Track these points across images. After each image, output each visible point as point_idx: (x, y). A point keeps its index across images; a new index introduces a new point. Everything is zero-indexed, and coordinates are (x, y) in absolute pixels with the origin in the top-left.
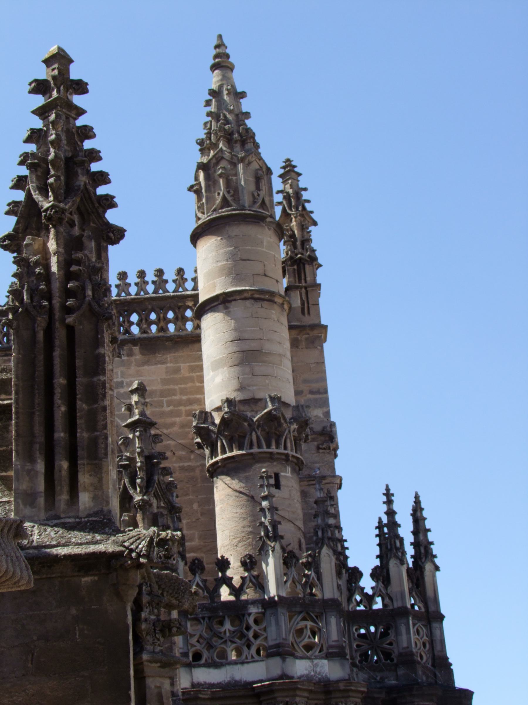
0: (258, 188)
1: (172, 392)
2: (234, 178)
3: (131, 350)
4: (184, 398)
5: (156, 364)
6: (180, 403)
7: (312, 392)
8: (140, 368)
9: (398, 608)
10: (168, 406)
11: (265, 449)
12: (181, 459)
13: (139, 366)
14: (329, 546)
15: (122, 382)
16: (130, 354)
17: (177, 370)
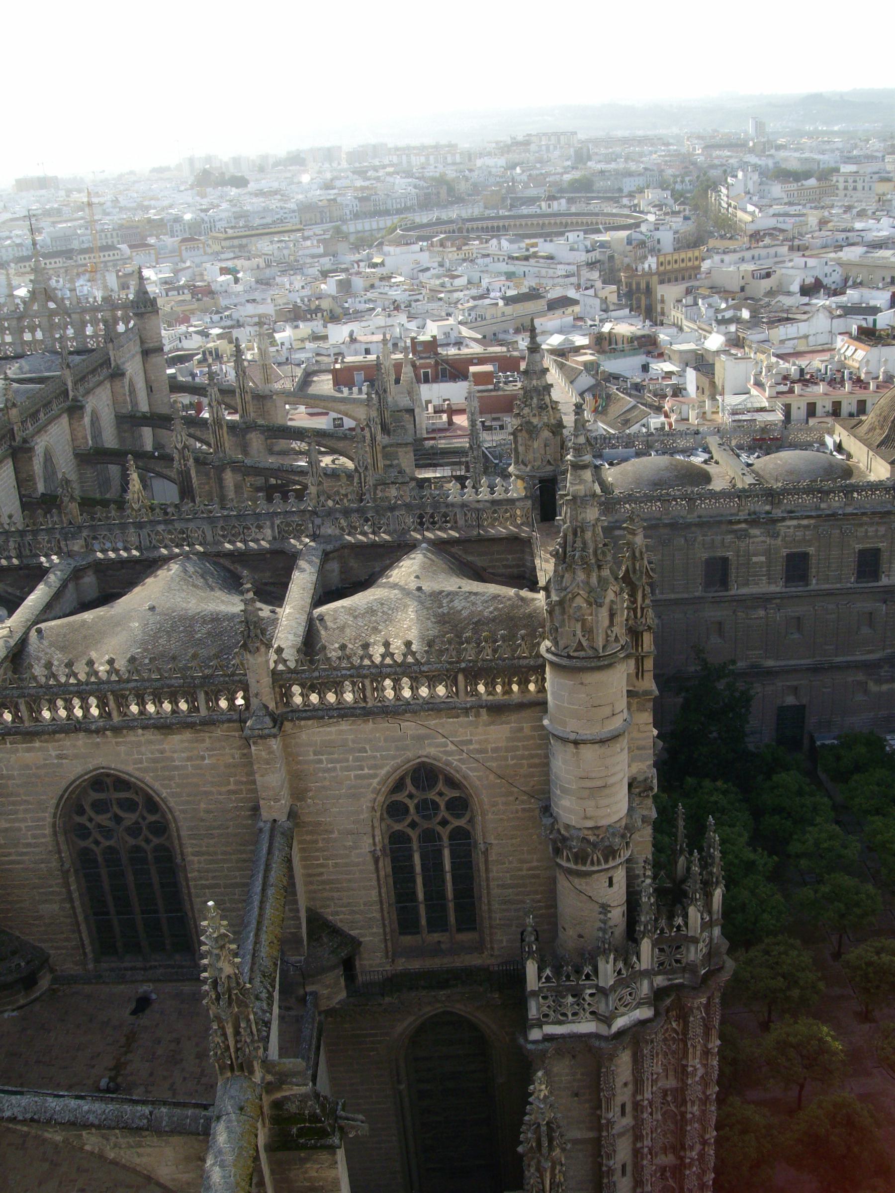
0: (612, 624)
1: (516, 748)
2: (590, 618)
3: (478, 712)
4: (526, 753)
5: (502, 724)
6: (522, 757)
7: (638, 748)
8: (488, 728)
9: (692, 937)
10: (512, 760)
11: (604, 866)
12: (523, 802)
13: (486, 725)
14: (649, 938)
15: (471, 740)
16: (477, 715)
17: (521, 729)
